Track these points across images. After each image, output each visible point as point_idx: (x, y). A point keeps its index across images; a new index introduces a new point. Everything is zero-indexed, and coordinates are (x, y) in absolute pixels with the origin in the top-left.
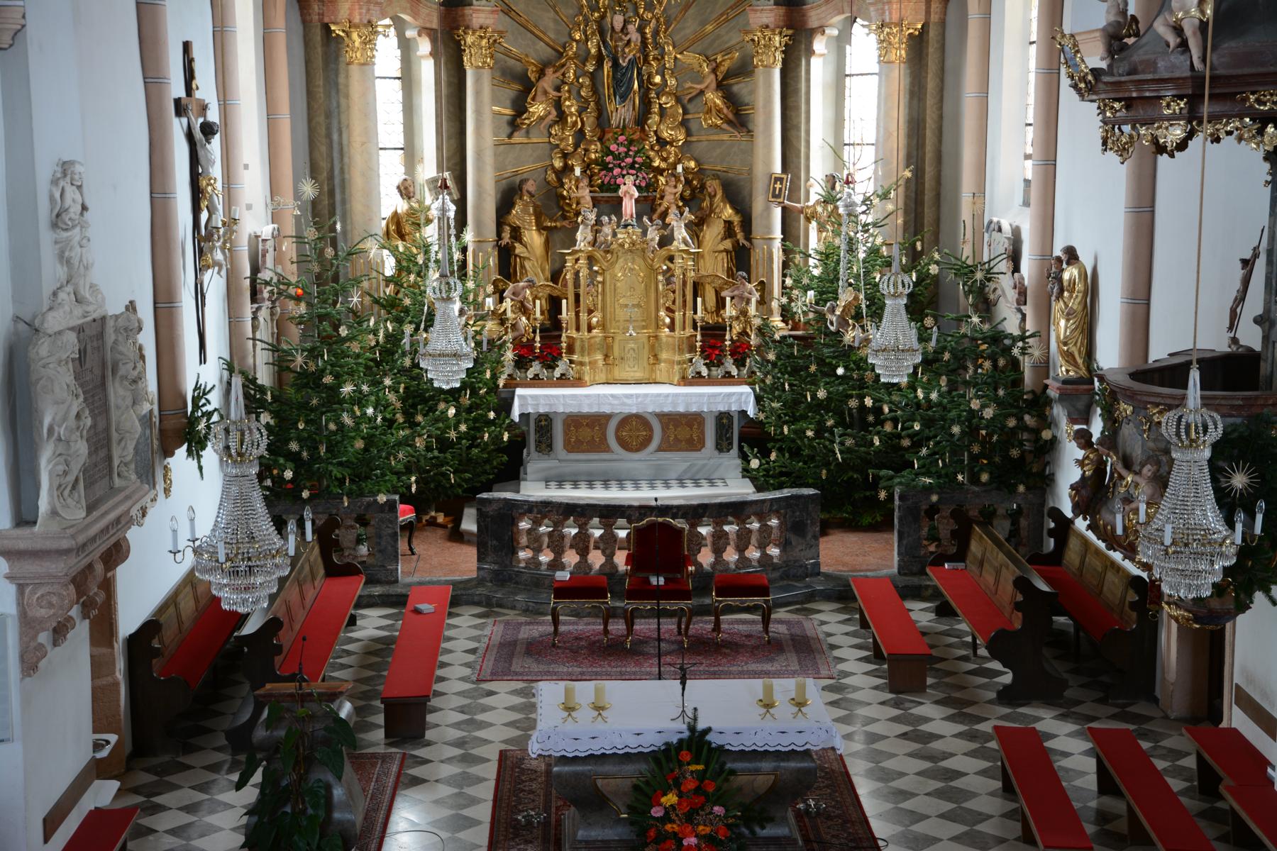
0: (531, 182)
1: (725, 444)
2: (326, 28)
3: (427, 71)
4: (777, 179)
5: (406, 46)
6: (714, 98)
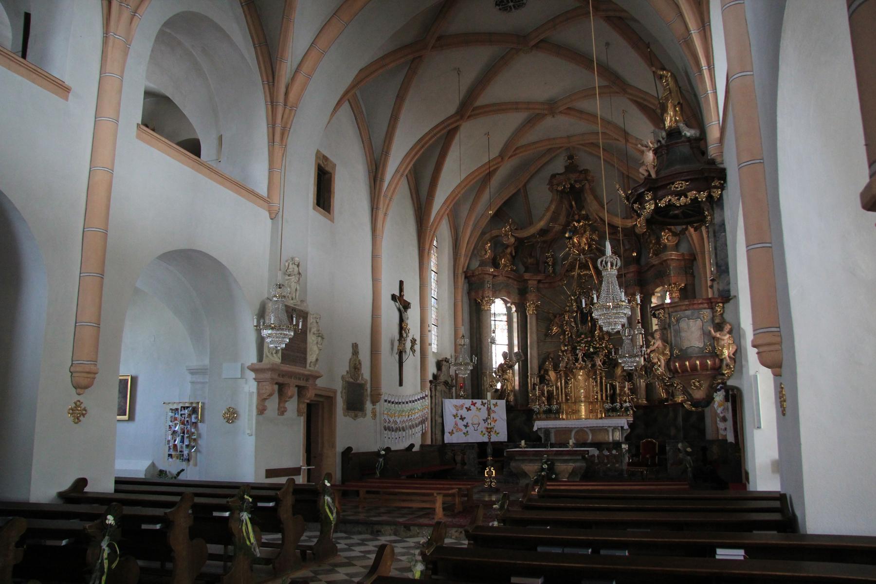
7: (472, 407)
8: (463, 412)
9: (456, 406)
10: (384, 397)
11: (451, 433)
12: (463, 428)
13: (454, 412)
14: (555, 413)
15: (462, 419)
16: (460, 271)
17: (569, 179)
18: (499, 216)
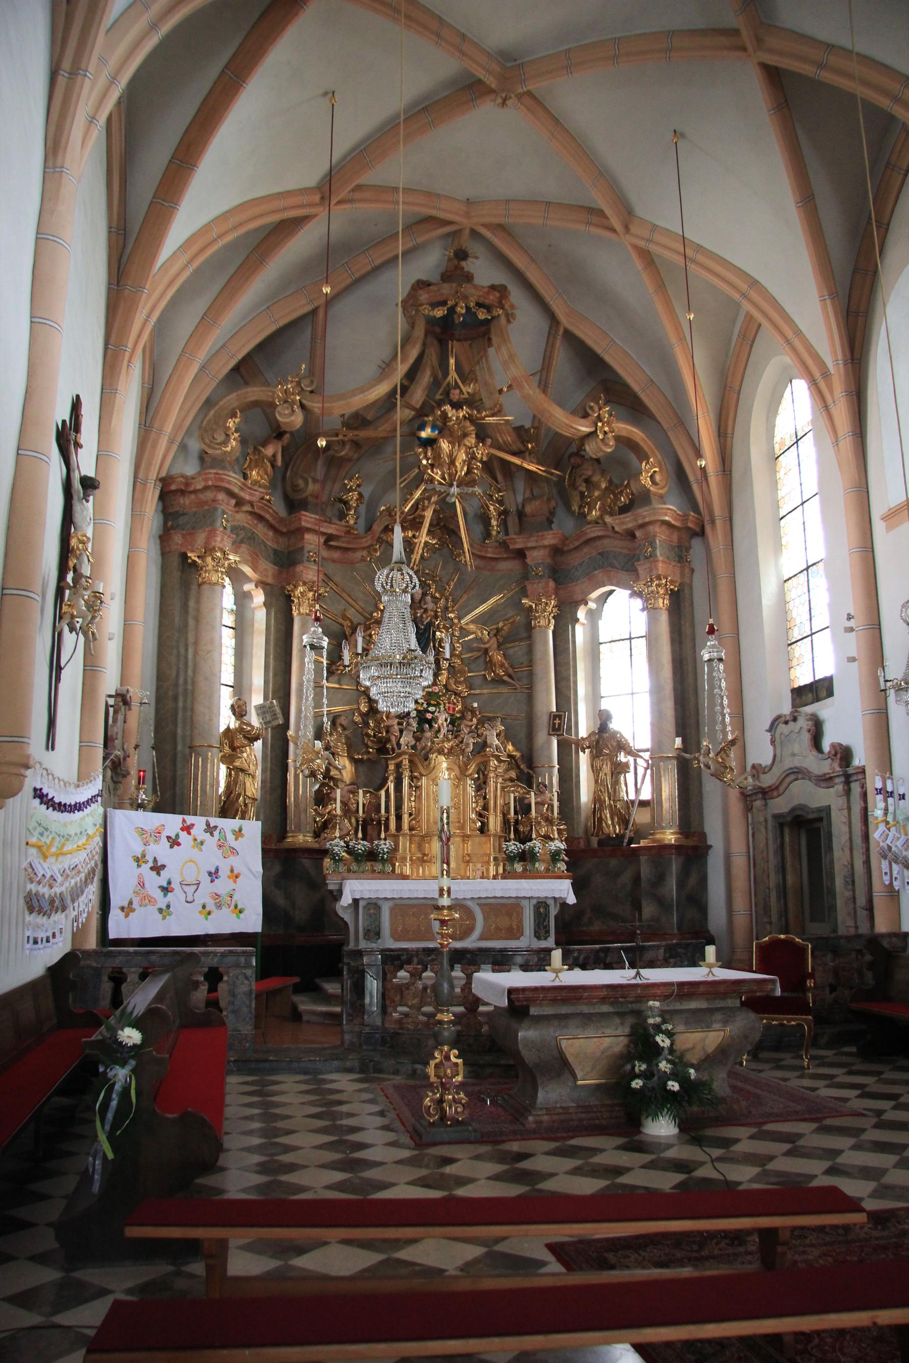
0: (342, 718)
1: (542, 932)
2: (184, 556)
3: (260, 617)
4: (555, 717)
5: (242, 598)
6: (498, 657)
7: (183, 835)
8: (160, 850)
9: (142, 832)
10: (33, 780)
11: (127, 909)
12: (158, 894)
13: (138, 849)
14: (383, 861)
15: (157, 868)
16: (153, 475)
17: (465, 298)
18: (244, 371)
